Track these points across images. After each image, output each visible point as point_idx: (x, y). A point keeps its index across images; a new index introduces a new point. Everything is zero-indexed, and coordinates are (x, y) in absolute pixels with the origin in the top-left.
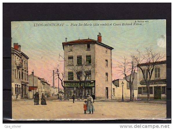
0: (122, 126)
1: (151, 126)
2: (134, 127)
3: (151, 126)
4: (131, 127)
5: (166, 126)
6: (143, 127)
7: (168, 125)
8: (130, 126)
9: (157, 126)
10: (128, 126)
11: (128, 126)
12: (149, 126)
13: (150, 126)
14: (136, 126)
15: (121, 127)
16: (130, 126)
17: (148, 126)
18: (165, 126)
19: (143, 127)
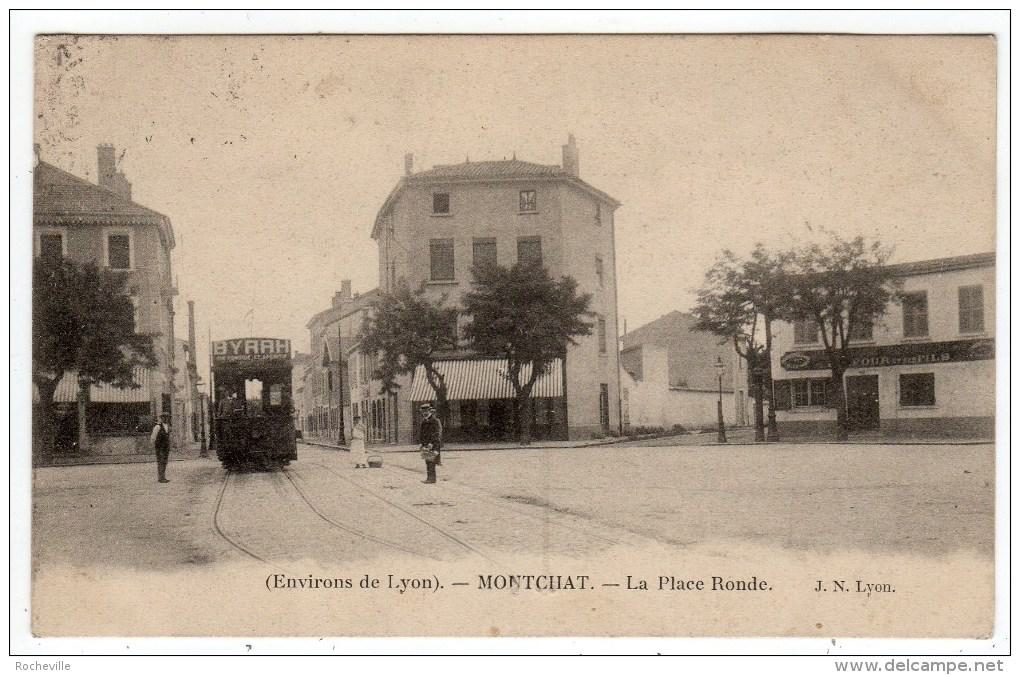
0: (842, 664)
1: (941, 666)
2: (883, 668)
3: (941, 666)
4: (875, 670)
5: (990, 666)
6: (915, 667)
7: (999, 663)
9: (959, 666)
10: (864, 666)
11: (864, 666)
12: (935, 666)
13: (938, 664)
14: (893, 664)
15: (839, 670)
16: (872, 664)
17: (932, 664)
18: (987, 666)
19: (915, 667)
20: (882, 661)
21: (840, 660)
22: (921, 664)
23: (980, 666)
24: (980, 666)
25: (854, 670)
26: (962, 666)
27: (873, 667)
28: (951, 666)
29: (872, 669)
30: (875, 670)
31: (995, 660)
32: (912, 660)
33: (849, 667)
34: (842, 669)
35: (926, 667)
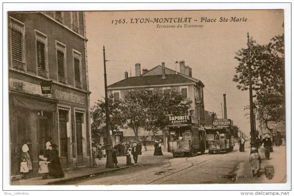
0: (243, 193)
1: (271, 193)
2: (255, 194)
3: (271, 193)
4: (252, 194)
5: (285, 193)
6: (264, 194)
7: (288, 192)
8: (243, 193)
9: (277, 193)
10: (249, 193)
11: (249, 193)
12: (270, 193)
13: (270, 193)
14: (257, 193)
15: (242, 194)
16: (251, 193)
17: (269, 193)
18: (285, 193)
19: (264, 194)
20: (254, 192)
21: (242, 192)
22: (265, 193)
23: (282, 194)
24: (282, 194)
25: (246, 194)
26: (277, 193)
27: (252, 194)
28: (274, 194)
29: (251, 194)
30: (252, 194)
31: (287, 192)
32: (263, 192)
33: (245, 194)
34: (243, 194)
35: (267, 194)
